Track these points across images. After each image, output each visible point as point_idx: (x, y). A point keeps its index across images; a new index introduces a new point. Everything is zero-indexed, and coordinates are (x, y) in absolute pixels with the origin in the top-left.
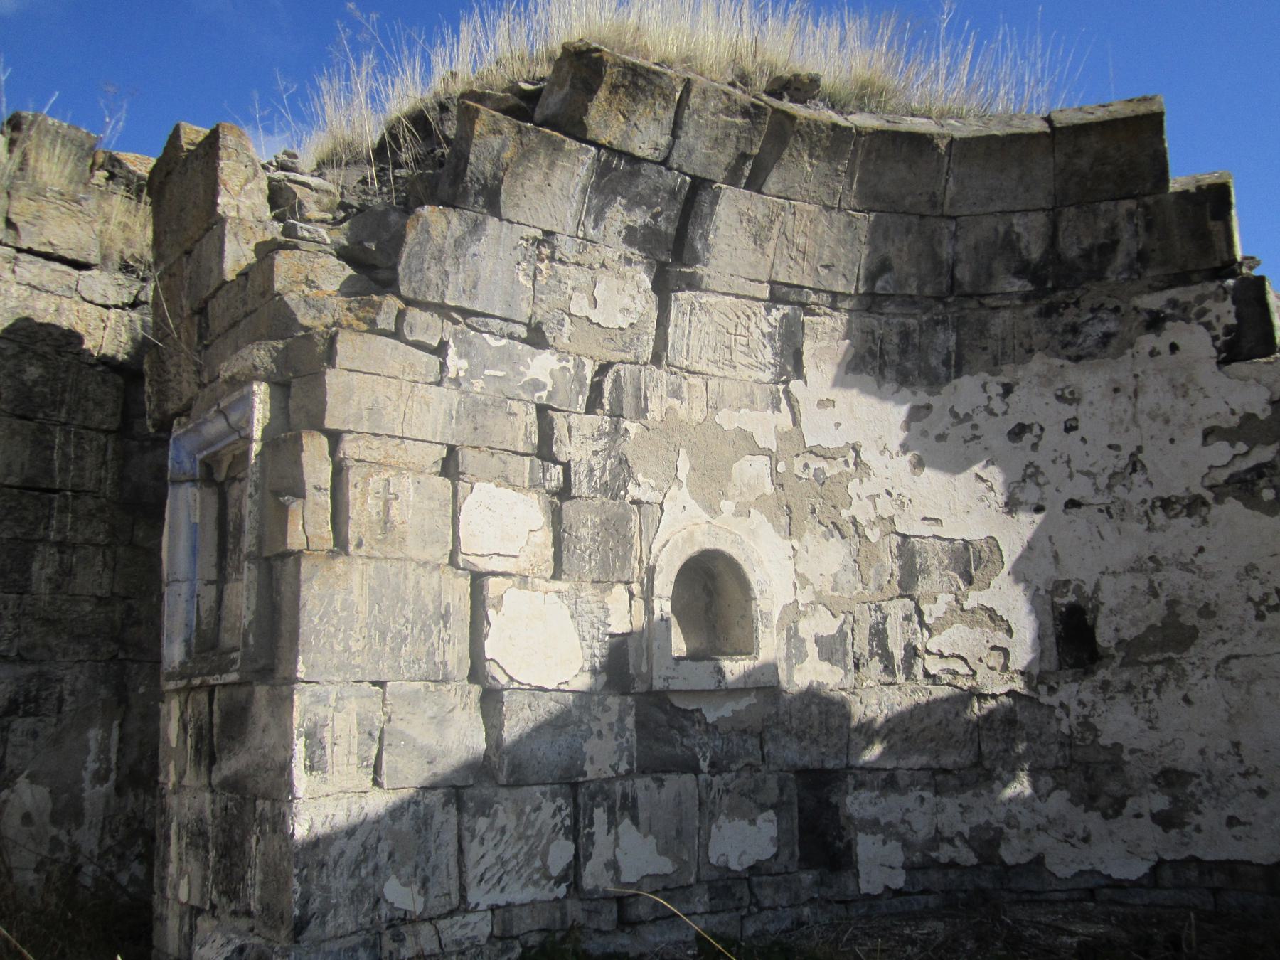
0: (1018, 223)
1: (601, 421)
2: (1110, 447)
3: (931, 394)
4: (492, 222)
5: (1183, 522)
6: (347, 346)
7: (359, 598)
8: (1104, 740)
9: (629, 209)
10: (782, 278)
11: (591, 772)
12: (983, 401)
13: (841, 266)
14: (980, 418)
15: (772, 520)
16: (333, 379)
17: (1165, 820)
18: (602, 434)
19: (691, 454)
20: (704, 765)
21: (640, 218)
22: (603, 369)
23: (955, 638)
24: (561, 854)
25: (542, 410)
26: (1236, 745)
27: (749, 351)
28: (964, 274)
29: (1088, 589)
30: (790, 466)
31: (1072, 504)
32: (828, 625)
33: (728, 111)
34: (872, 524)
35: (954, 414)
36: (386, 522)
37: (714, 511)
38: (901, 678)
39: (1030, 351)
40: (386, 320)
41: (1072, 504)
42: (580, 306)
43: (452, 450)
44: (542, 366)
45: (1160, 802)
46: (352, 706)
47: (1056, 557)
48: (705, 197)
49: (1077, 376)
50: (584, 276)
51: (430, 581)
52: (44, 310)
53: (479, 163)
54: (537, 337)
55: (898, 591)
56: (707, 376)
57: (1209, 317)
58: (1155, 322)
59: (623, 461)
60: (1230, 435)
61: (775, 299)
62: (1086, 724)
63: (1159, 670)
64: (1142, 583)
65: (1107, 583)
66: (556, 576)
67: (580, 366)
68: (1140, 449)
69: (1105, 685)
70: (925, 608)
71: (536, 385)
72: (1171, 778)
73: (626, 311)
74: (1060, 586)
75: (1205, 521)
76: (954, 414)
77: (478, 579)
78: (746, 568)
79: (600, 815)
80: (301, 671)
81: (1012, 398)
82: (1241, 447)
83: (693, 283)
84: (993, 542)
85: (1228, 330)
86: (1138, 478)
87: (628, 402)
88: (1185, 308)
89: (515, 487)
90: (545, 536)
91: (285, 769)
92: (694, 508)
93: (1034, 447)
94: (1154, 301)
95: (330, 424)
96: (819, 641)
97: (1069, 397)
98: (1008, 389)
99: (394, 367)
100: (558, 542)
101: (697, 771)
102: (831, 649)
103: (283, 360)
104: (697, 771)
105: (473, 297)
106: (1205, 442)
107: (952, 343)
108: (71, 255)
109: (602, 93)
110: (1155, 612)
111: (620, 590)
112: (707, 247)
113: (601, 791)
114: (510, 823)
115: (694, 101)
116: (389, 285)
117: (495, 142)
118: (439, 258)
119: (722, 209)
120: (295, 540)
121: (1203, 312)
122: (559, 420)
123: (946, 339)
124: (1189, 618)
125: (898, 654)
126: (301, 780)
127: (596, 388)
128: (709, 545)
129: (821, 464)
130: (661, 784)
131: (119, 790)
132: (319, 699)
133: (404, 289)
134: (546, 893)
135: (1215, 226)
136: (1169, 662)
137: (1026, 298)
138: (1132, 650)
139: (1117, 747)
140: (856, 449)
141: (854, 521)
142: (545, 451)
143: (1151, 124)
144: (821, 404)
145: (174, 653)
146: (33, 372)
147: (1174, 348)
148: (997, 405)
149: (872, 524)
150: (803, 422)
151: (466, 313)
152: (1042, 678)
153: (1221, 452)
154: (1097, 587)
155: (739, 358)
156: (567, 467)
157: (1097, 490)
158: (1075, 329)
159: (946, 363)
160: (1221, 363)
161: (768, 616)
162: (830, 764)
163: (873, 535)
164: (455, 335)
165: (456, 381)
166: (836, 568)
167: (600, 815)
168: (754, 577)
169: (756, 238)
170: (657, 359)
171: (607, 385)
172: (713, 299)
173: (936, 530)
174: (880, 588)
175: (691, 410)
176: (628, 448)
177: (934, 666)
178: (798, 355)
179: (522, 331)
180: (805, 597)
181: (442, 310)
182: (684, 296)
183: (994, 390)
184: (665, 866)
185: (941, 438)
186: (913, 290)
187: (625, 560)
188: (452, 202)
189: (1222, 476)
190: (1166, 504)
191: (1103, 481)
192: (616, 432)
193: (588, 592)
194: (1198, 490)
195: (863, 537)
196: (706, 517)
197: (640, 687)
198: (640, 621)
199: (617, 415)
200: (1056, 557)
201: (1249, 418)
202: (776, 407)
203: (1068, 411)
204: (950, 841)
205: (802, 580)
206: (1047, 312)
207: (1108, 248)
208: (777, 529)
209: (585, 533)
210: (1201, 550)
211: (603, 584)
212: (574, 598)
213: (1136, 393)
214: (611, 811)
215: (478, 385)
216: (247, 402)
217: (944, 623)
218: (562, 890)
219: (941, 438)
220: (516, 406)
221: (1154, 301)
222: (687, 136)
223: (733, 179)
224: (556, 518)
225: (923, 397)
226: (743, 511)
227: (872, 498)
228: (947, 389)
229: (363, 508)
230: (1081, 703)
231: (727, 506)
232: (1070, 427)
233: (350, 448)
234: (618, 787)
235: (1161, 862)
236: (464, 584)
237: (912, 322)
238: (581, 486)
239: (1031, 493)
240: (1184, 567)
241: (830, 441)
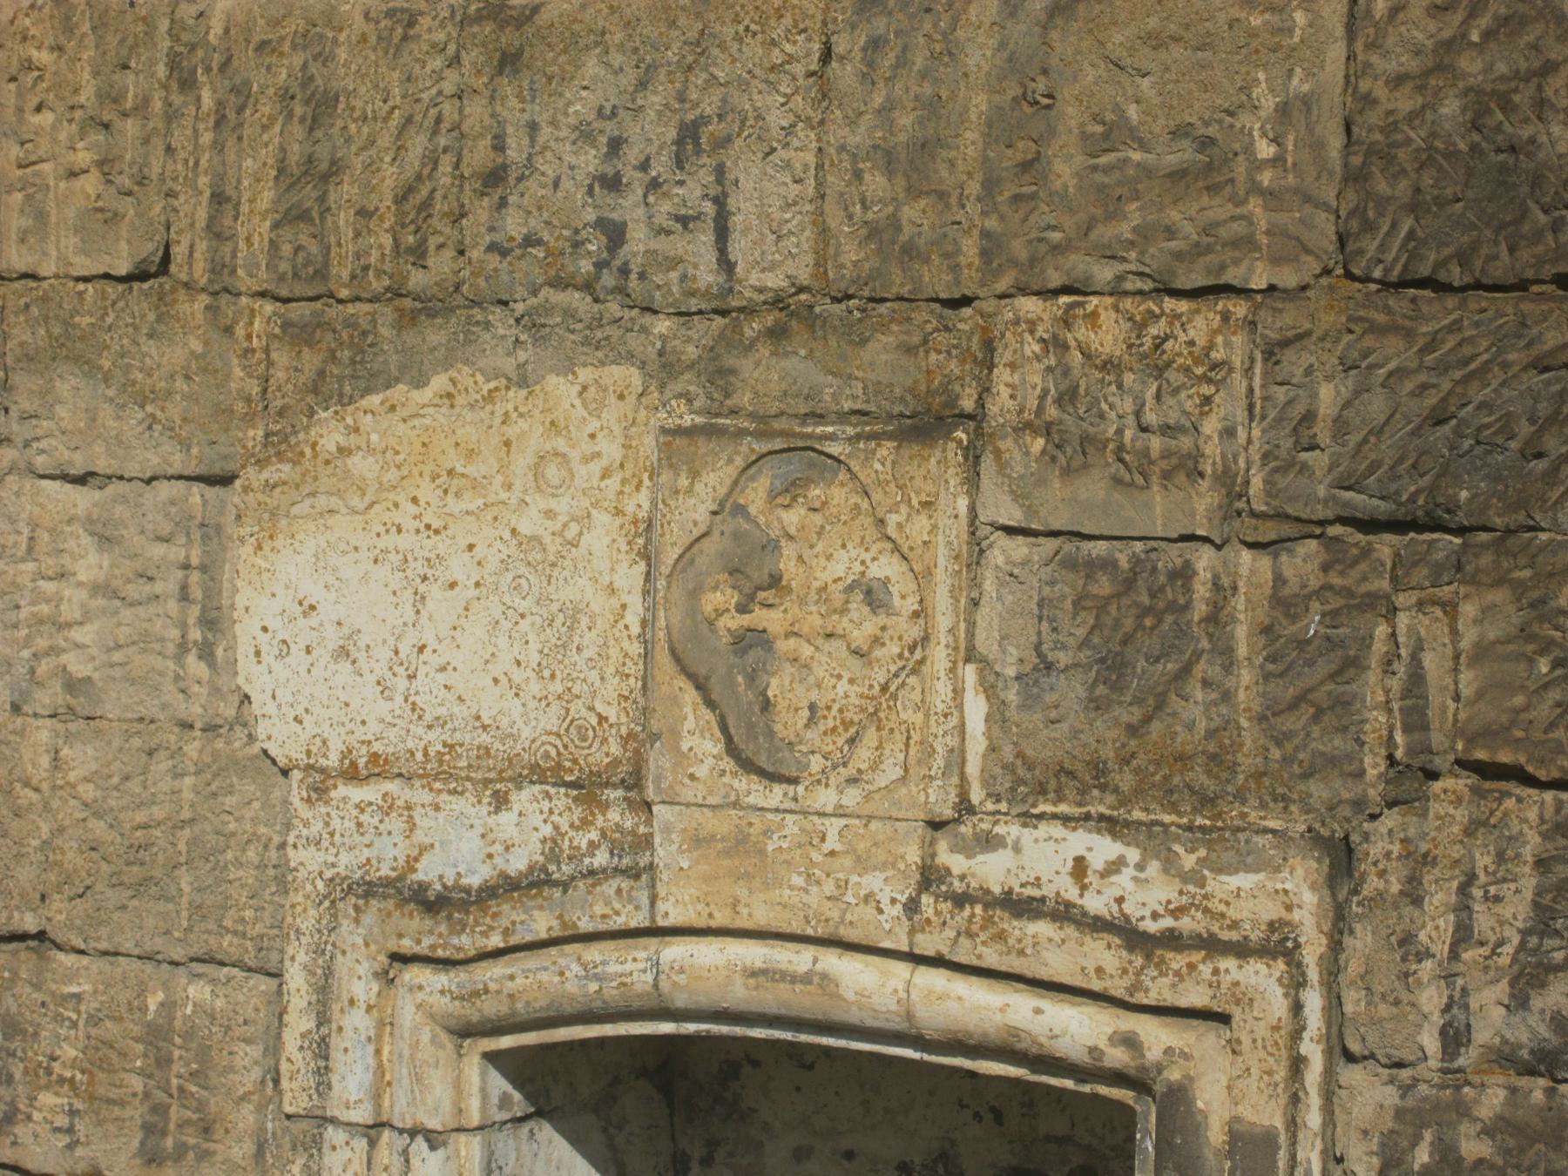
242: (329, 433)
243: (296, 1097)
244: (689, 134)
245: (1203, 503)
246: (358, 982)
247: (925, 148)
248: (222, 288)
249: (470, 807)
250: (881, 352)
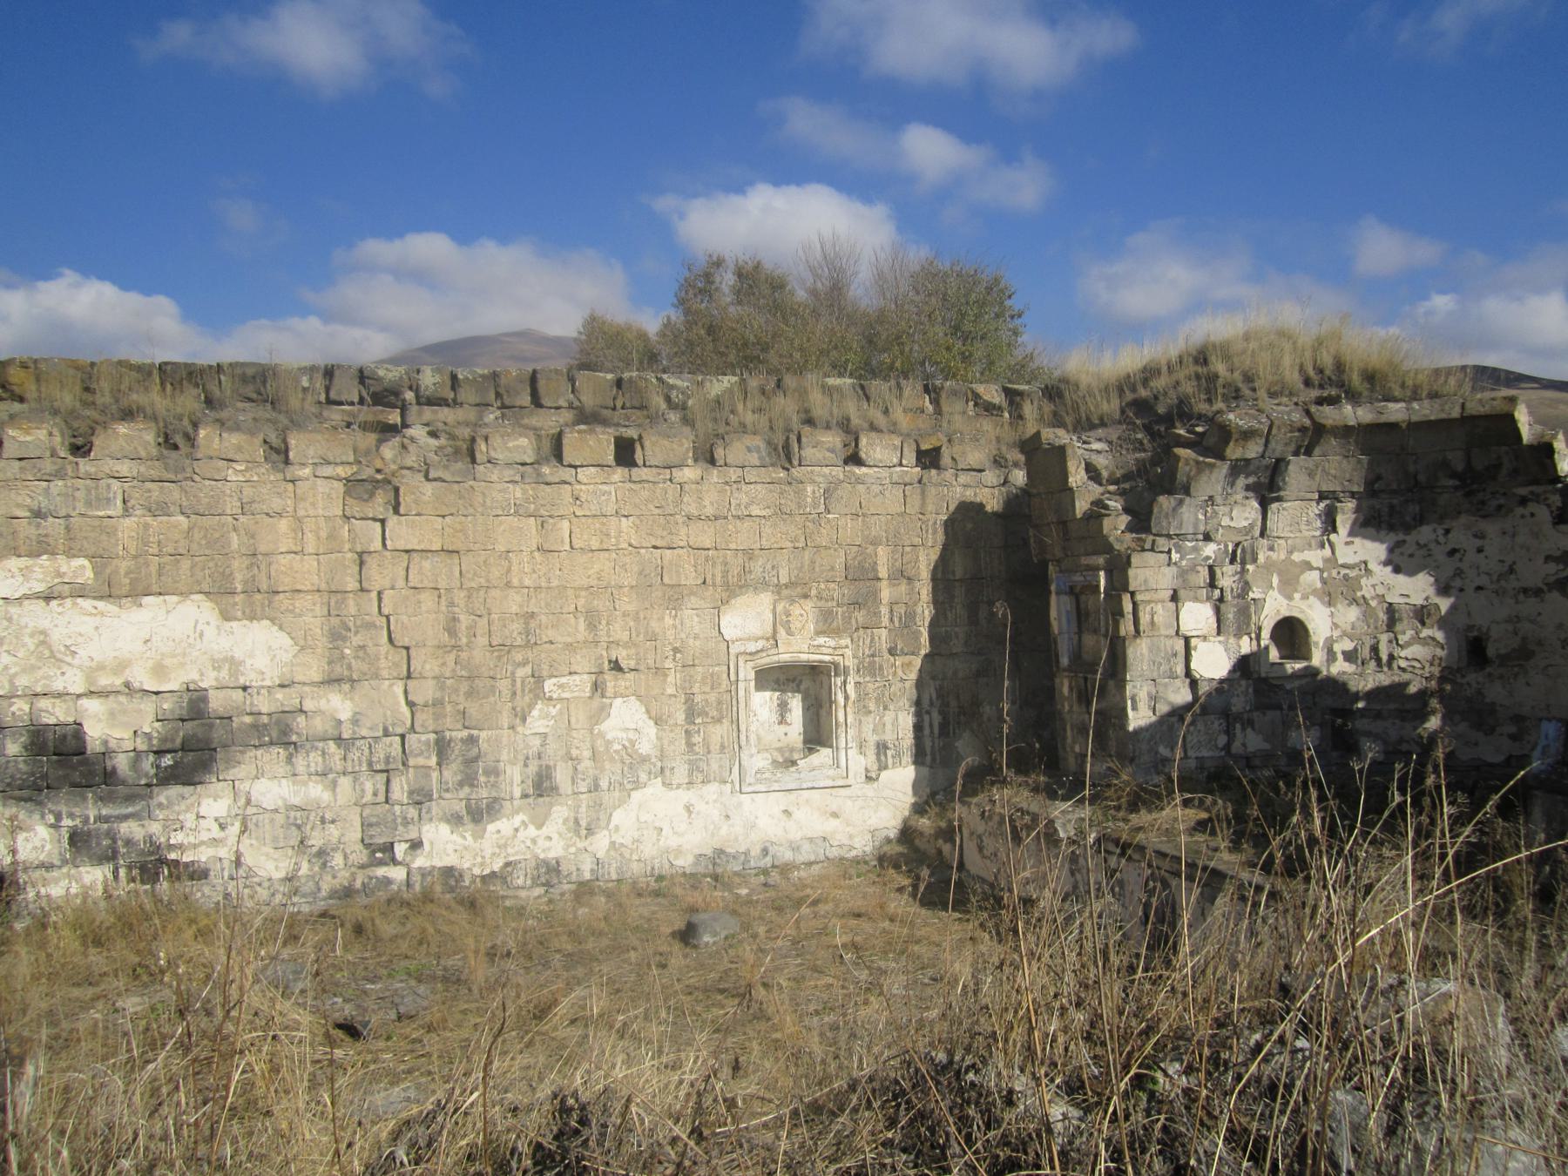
0: (1450, 456)
1: (1237, 567)
2: (1500, 561)
3: (1406, 534)
4: (1188, 499)
5: (1533, 600)
6: (1135, 559)
7: (1145, 651)
8: (1488, 700)
9: (1246, 477)
10: (1324, 489)
11: (1234, 709)
12: (1433, 537)
13: (1356, 479)
14: (1432, 546)
15: (1320, 599)
16: (1131, 572)
17: (1513, 737)
18: (1237, 573)
19: (1279, 575)
20: (1285, 707)
21: (1251, 480)
22: (1237, 545)
23: (1415, 651)
24: (1222, 740)
25: (1211, 568)
26: (1548, 706)
27: (1308, 523)
28: (1422, 478)
29: (1484, 630)
30: (1330, 574)
32: (1348, 645)
33: (1291, 432)
34: (1373, 598)
35: (1418, 544)
36: (1152, 623)
37: (1290, 598)
38: (1385, 669)
39: (1460, 513)
40: (1148, 546)
41: (1479, 588)
42: (1225, 521)
43: (1175, 591)
44: (1210, 550)
45: (1513, 729)
46: (1145, 689)
47: (1469, 614)
48: (1283, 464)
49: (1484, 525)
50: (1227, 509)
51: (1169, 642)
52: (969, 495)
53: (1181, 477)
54: (1207, 538)
55: (1385, 628)
56: (1286, 539)
57: (1549, 502)
58: (1523, 501)
59: (1247, 583)
60: (1556, 560)
61: (1322, 496)
62: (1479, 692)
63: (1516, 669)
64: (1510, 628)
66: (1219, 634)
67: (1226, 546)
68: (1514, 563)
69: (1490, 675)
70: (1400, 637)
71: (1208, 558)
72: (1518, 719)
73: (1246, 519)
74: (1470, 628)
75: (1542, 601)
76: (1418, 544)
77: (1187, 640)
78: (1306, 623)
79: (1238, 726)
80: (1128, 677)
81: (1450, 536)
82: (1561, 567)
83: (1279, 499)
84: (1437, 607)
85: (1559, 508)
86: (1513, 577)
87: (1248, 557)
88: (1538, 495)
89: (1201, 602)
90: (1213, 620)
91: (1125, 709)
92: (1280, 598)
93: (1461, 560)
94: (1523, 491)
95: (1131, 589)
96: (1344, 653)
97: (1480, 536)
98: (1447, 531)
99: (1152, 563)
100: (1219, 621)
101: (1281, 709)
102: (1349, 656)
103: (1107, 562)
104: (1281, 709)
105: (1180, 529)
106: (1546, 562)
107: (1417, 508)
108: (978, 467)
109: (1231, 444)
111: (1246, 638)
112: (1285, 483)
113: (1238, 717)
114: (1202, 728)
115: (1274, 431)
116: (1147, 530)
117: (1187, 468)
118: (1167, 516)
119: (1291, 467)
120: (1122, 633)
121: (1546, 499)
122: (1218, 571)
123: (1414, 508)
125: (1384, 658)
126: (1130, 713)
127: (1234, 552)
128: (1287, 614)
129: (1347, 571)
130: (1264, 714)
131: (1021, 708)
132: (1134, 687)
133: (1154, 531)
134: (1217, 754)
136: (1521, 666)
137: (1456, 488)
138: (1504, 659)
139: (1493, 704)
140: (1365, 563)
141: (1363, 597)
142: (1212, 584)
144: (1347, 543)
145: (1065, 661)
146: (970, 526)
148: (1442, 539)
149: (1373, 598)
150: (1337, 553)
151: (1177, 535)
152: (1459, 670)
153: (1552, 568)
154: (1489, 629)
155: (1303, 527)
156: (1222, 590)
157: (1492, 582)
158: (1483, 503)
159: (1414, 519)
161: (1317, 644)
162: (1348, 707)
163: (1373, 603)
164: (1174, 545)
165: (1175, 564)
166: (1353, 619)
167: (1238, 726)
168: (1310, 627)
169: (1309, 475)
170: (1262, 535)
171: (1239, 551)
172: (1289, 504)
173: (1407, 600)
174: (1376, 628)
175: (1279, 555)
176: (1249, 577)
177: (1403, 664)
178: (1334, 522)
179: (1201, 537)
180: (1336, 634)
181: (1169, 536)
182: (1274, 506)
183: (1440, 531)
184: (1267, 746)
185: (1411, 556)
186: (1395, 486)
187: (1248, 625)
188: (1170, 492)
189: (1552, 579)
190: (1525, 591)
191: (1495, 578)
192: (1243, 571)
193: (1232, 640)
194: (1540, 585)
195: (1368, 604)
196: (1286, 602)
197: (1255, 676)
198: (1255, 648)
199: (1243, 563)
200: (1469, 614)
202: (1323, 546)
203: (1479, 543)
204: (1408, 742)
205: (1335, 625)
206: (1468, 494)
207: (1498, 466)
208: (1323, 603)
209: (1231, 616)
210: (1540, 614)
211: (1238, 636)
212: (1225, 644)
213: (1514, 536)
214: (1243, 725)
215: (1184, 563)
216: (1098, 576)
217: (1408, 644)
218: (1223, 753)
219: (1411, 556)
220: (1199, 568)
221: (1523, 491)
222: (1272, 444)
223: (1296, 453)
224: (1218, 611)
225: (1401, 537)
226: (1305, 597)
227: (1373, 586)
228: (1414, 533)
229: (1144, 619)
230: (1478, 683)
231: (1297, 596)
232: (1480, 550)
233: (1139, 597)
234: (1245, 716)
235: (1511, 756)
236: (1182, 642)
237: (1395, 501)
238: (1228, 596)
239: (1457, 583)
240: (1533, 622)
241: (1351, 560)
242: (733, 601)
243: (733, 678)
244: (773, 567)
245: (835, 604)
246: (741, 663)
247: (802, 567)
248: (714, 585)
249: (753, 643)
250: (799, 589)
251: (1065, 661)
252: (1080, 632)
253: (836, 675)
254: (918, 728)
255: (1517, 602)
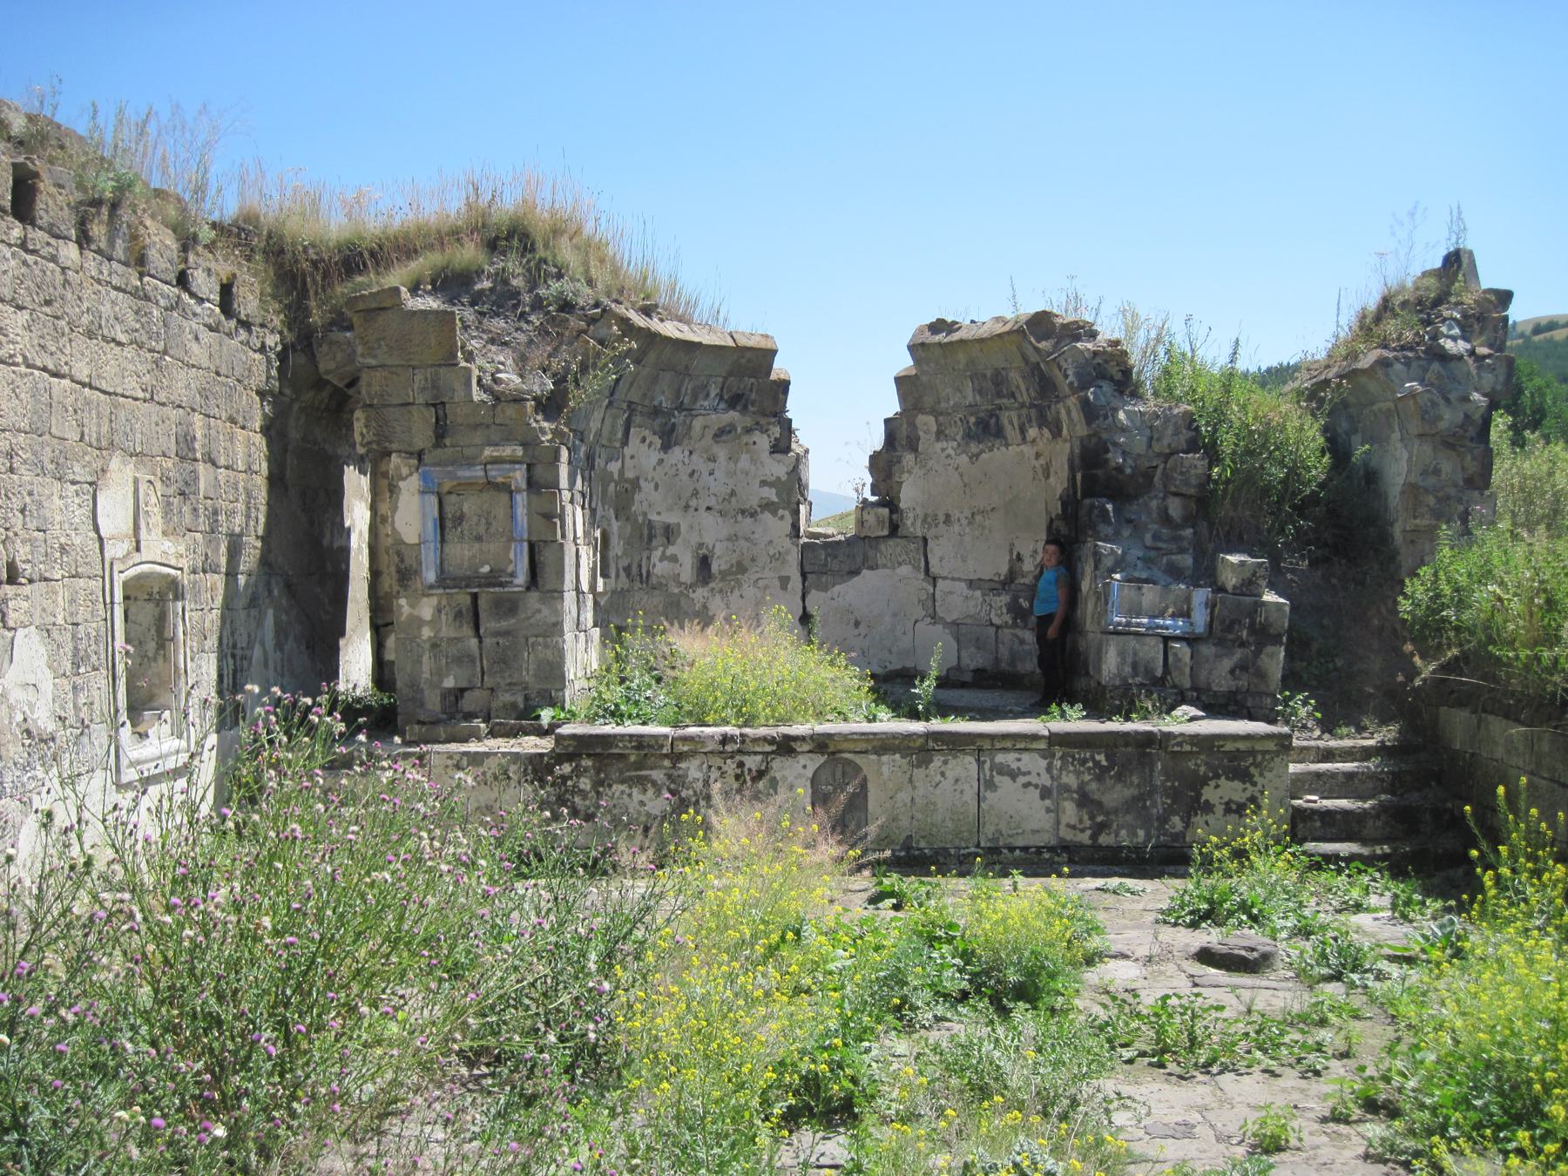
5: (749, 520)
14: (680, 465)
31: (709, 508)
41: (709, 508)
65: (718, 545)
69: (713, 589)
85: (776, 439)
86: (733, 499)
110: (734, 558)
124: (746, 563)
135: (781, 396)
138: (724, 575)
143: (774, 352)
147: (755, 443)
160: (772, 453)
190: (743, 512)
191: (720, 500)
201: (778, 478)
203: (711, 465)
240: (747, 539)
243: (108, 600)
251: (430, 576)
252: (443, 541)
253: (176, 598)
254: (220, 677)
255: (736, 522)
